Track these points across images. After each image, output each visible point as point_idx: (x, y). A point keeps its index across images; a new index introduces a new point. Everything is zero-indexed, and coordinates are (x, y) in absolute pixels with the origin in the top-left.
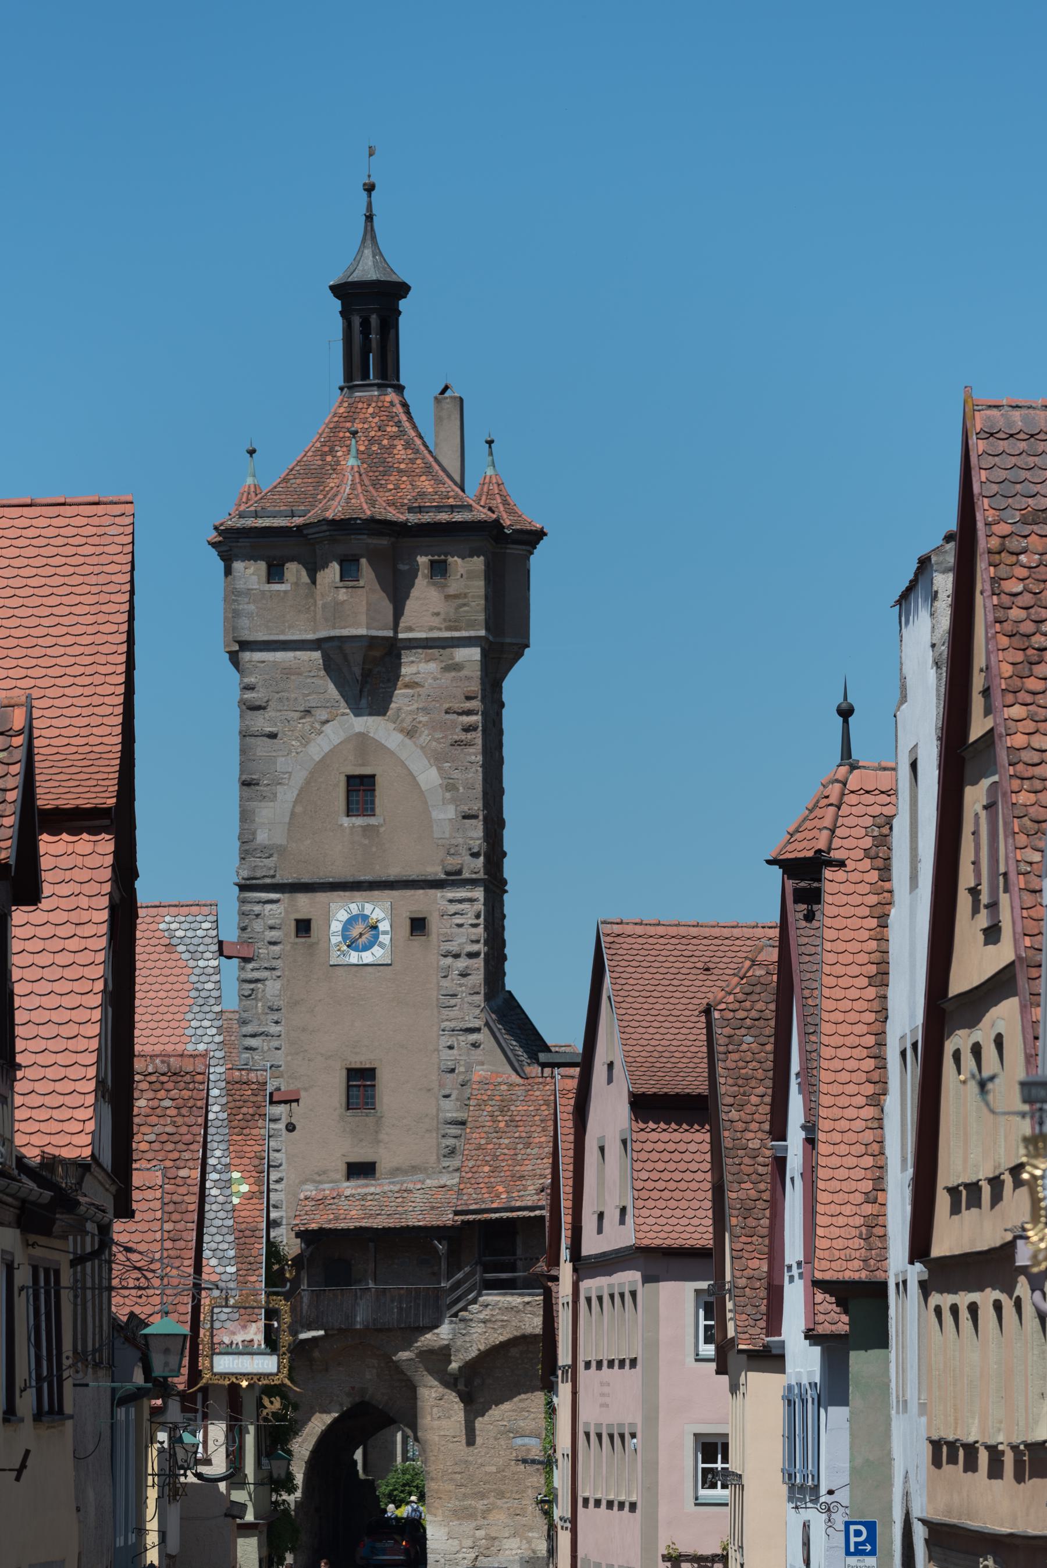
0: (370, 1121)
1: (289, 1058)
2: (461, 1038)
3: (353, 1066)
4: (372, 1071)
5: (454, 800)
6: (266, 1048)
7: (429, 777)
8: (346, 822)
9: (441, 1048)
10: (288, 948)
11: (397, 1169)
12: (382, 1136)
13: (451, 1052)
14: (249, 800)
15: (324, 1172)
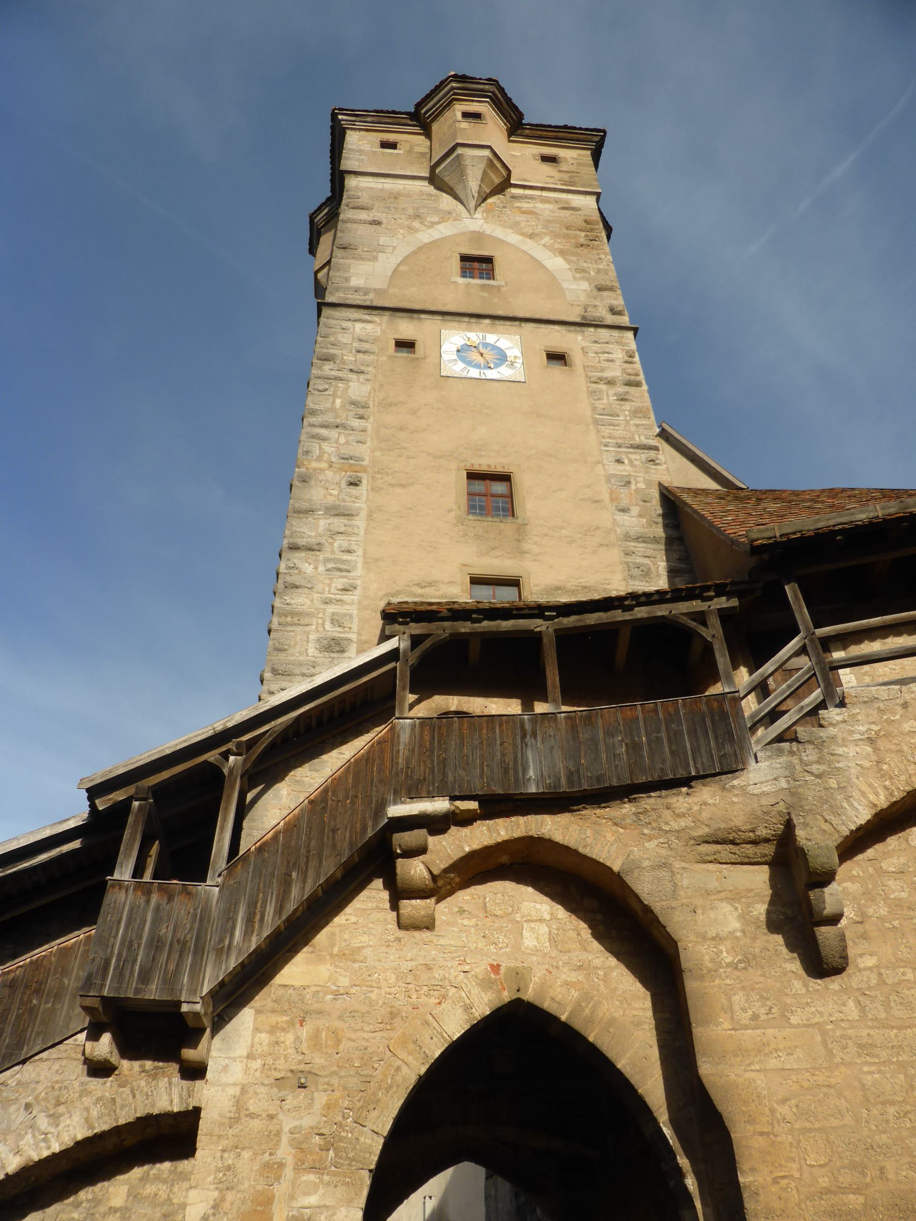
0: (507, 527)
1: (378, 454)
2: (632, 457)
3: (476, 467)
4: (505, 478)
5: (587, 279)
6: (342, 440)
7: (556, 264)
8: (461, 281)
9: (605, 461)
10: (385, 358)
11: (558, 588)
12: (526, 546)
13: (621, 467)
14: (343, 258)
15: (430, 584)
